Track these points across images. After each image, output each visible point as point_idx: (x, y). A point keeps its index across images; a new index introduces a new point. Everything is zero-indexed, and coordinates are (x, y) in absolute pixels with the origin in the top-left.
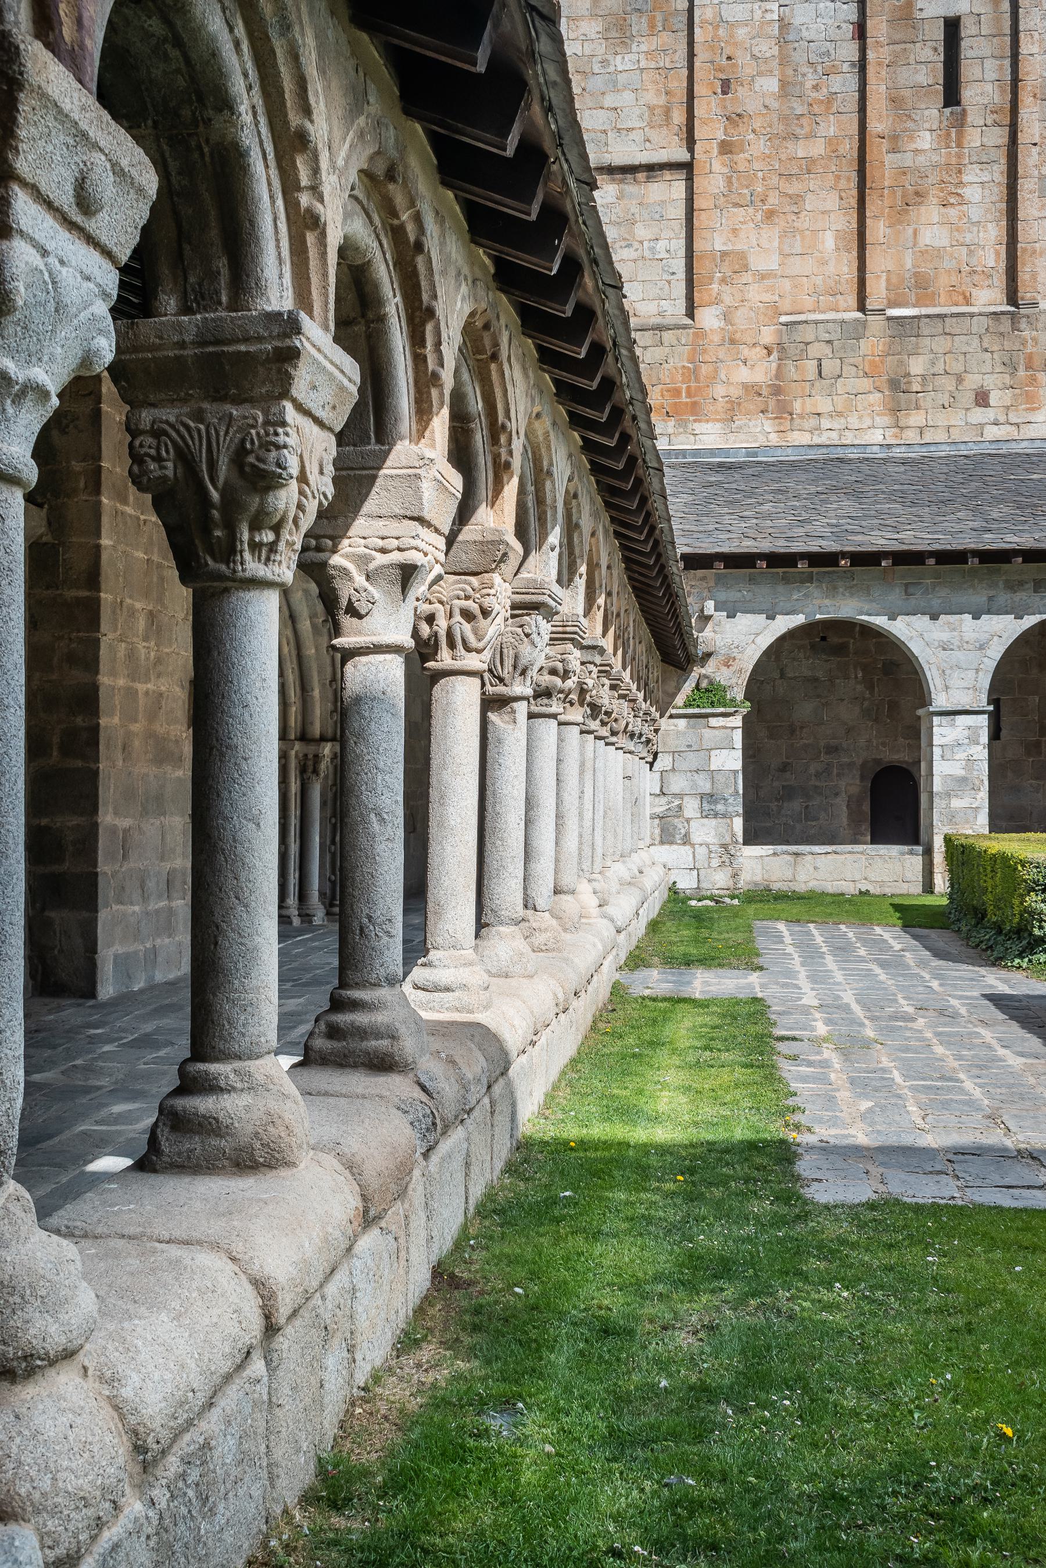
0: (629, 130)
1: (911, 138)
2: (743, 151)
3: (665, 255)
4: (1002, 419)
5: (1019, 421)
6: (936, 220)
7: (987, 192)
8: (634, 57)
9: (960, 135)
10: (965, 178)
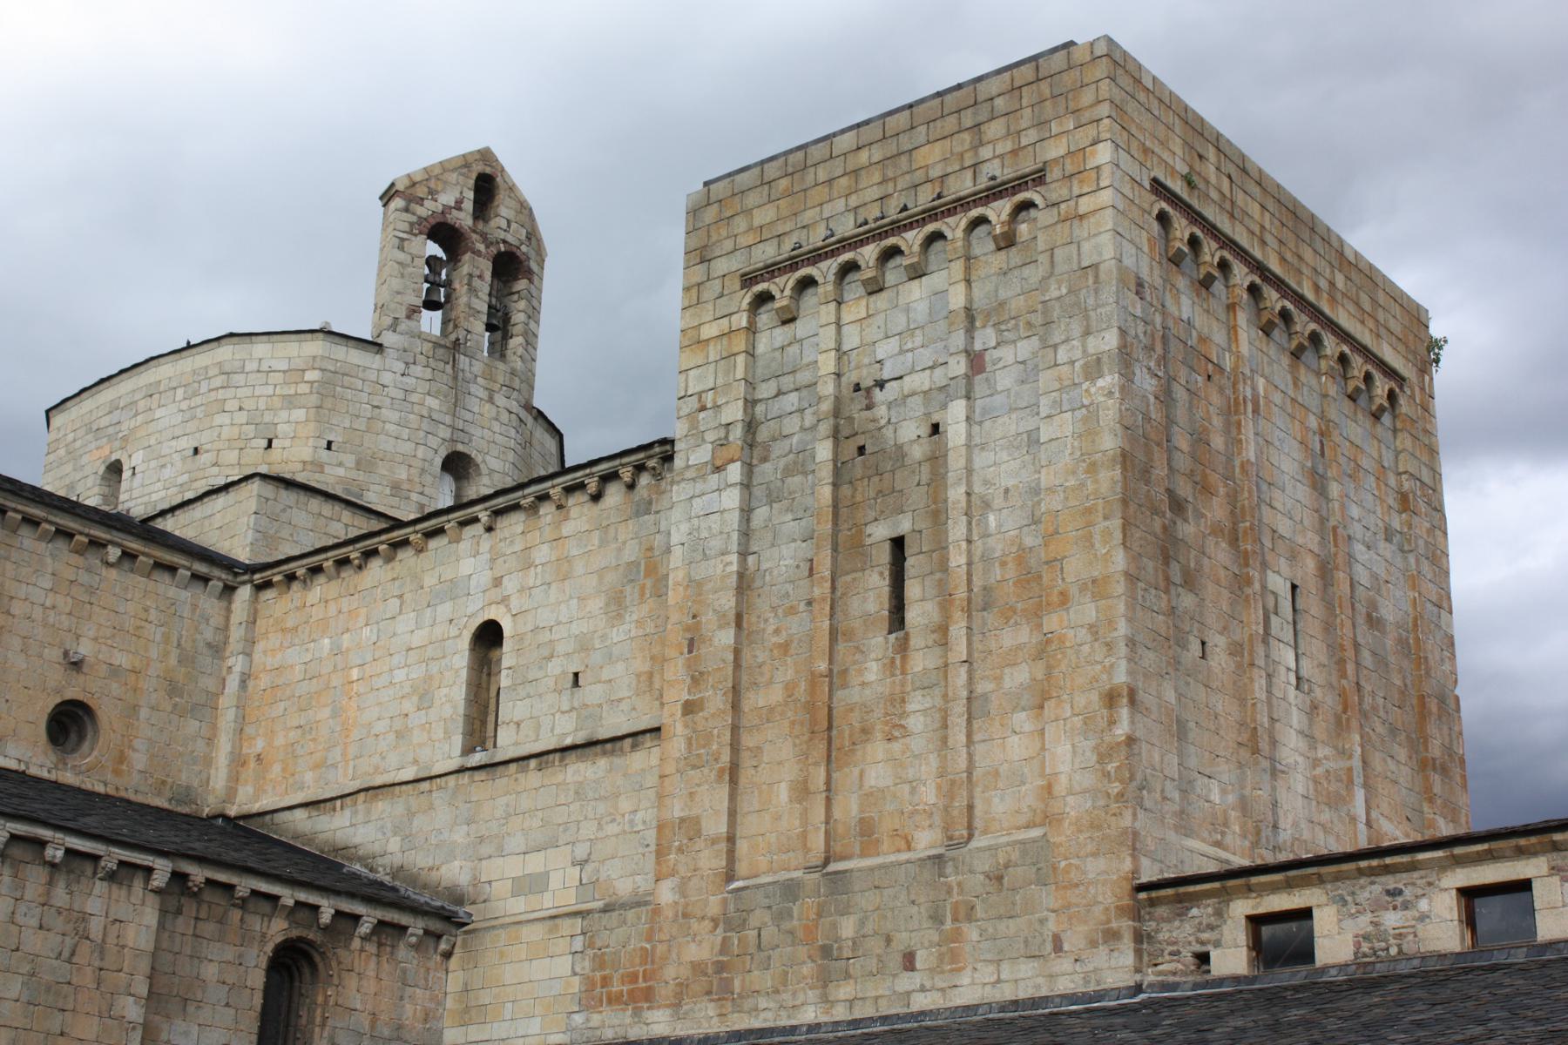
0: (620, 700)
1: (860, 672)
2: (702, 710)
3: (640, 827)
4: (928, 985)
5: (944, 985)
6: (880, 758)
7: (929, 719)
8: (626, 627)
9: (904, 659)
10: (910, 707)
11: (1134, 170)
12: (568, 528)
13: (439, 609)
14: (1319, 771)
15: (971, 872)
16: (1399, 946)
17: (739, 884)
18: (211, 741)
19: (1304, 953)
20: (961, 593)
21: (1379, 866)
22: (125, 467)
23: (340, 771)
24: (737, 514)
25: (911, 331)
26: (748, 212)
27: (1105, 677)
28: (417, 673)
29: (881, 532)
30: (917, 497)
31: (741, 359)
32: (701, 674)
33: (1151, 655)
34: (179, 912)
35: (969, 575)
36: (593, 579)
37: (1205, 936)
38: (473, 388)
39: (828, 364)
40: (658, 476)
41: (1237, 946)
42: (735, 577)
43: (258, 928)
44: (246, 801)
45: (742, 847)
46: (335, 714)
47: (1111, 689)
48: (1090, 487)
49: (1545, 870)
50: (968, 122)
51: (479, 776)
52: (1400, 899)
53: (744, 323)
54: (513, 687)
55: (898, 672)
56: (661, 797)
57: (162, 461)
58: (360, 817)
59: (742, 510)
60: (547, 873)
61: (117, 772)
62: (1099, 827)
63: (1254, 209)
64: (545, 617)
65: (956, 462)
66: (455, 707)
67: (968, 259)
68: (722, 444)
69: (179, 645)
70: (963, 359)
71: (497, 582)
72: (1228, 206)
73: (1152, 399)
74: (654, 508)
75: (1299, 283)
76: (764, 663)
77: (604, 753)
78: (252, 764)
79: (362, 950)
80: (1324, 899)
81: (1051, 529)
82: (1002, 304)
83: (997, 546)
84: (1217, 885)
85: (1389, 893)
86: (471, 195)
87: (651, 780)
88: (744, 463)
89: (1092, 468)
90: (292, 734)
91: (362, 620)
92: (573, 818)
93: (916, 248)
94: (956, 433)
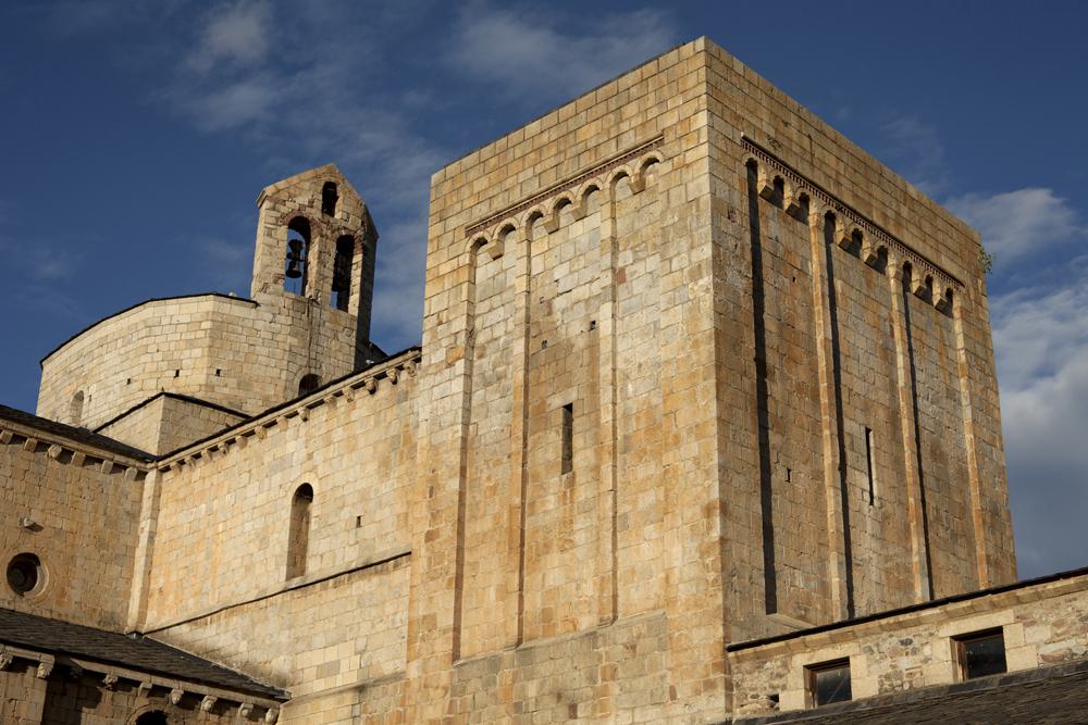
0: (387, 534)
1: (543, 504)
2: (438, 537)
7: (589, 534)
9: (572, 491)
10: (576, 526)
11: (728, 131)
12: (355, 415)
13: (273, 478)
14: (889, 565)
15: (615, 643)
16: (910, 682)
17: (461, 662)
18: (129, 580)
19: (844, 689)
20: (609, 442)
21: (894, 623)
22: (85, 396)
23: (210, 597)
24: (461, 395)
25: (577, 257)
26: (470, 184)
27: (704, 495)
28: (259, 524)
29: (557, 402)
30: (581, 375)
31: (465, 286)
32: (438, 512)
33: (741, 478)
34: (64, 694)
35: (614, 427)
36: (370, 450)
37: (776, 682)
38: (322, 331)
39: (521, 285)
40: (412, 373)
41: (798, 689)
42: (460, 441)
43: (125, 704)
44: (153, 620)
45: (464, 635)
46: (208, 556)
47: (709, 504)
48: (694, 358)
49: (1012, 619)
50: (613, 107)
51: (297, 594)
52: (910, 647)
53: (467, 262)
54: (318, 531)
55: (568, 502)
56: (411, 602)
57: (108, 390)
58: (222, 629)
59: (465, 393)
60: (339, 661)
61: (59, 603)
62: (701, 606)
63: (831, 161)
64: (339, 479)
65: (605, 348)
66: (282, 547)
67: (613, 203)
68: (452, 348)
69: (105, 514)
70: (610, 273)
71: (310, 456)
72: (808, 157)
73: (742, 293)
74: (410, 396)
75: (869, 213)
76: (480, 501)
77: (376, 573)
78: (156, 595)
79: (207, 720)
80: (857, 650)
81: (668, 390)
82: (639, 230)
83: (633, 406)
84: (782, 643)
85: (902, 643)
86: (321, 197)
87: (406, 590)
88: (467, 359)
89: (696, 344)
90: (181, 572)
91: (225, 490)
92: (356, 621)
93: (579, 198)
94: (605, 327)
